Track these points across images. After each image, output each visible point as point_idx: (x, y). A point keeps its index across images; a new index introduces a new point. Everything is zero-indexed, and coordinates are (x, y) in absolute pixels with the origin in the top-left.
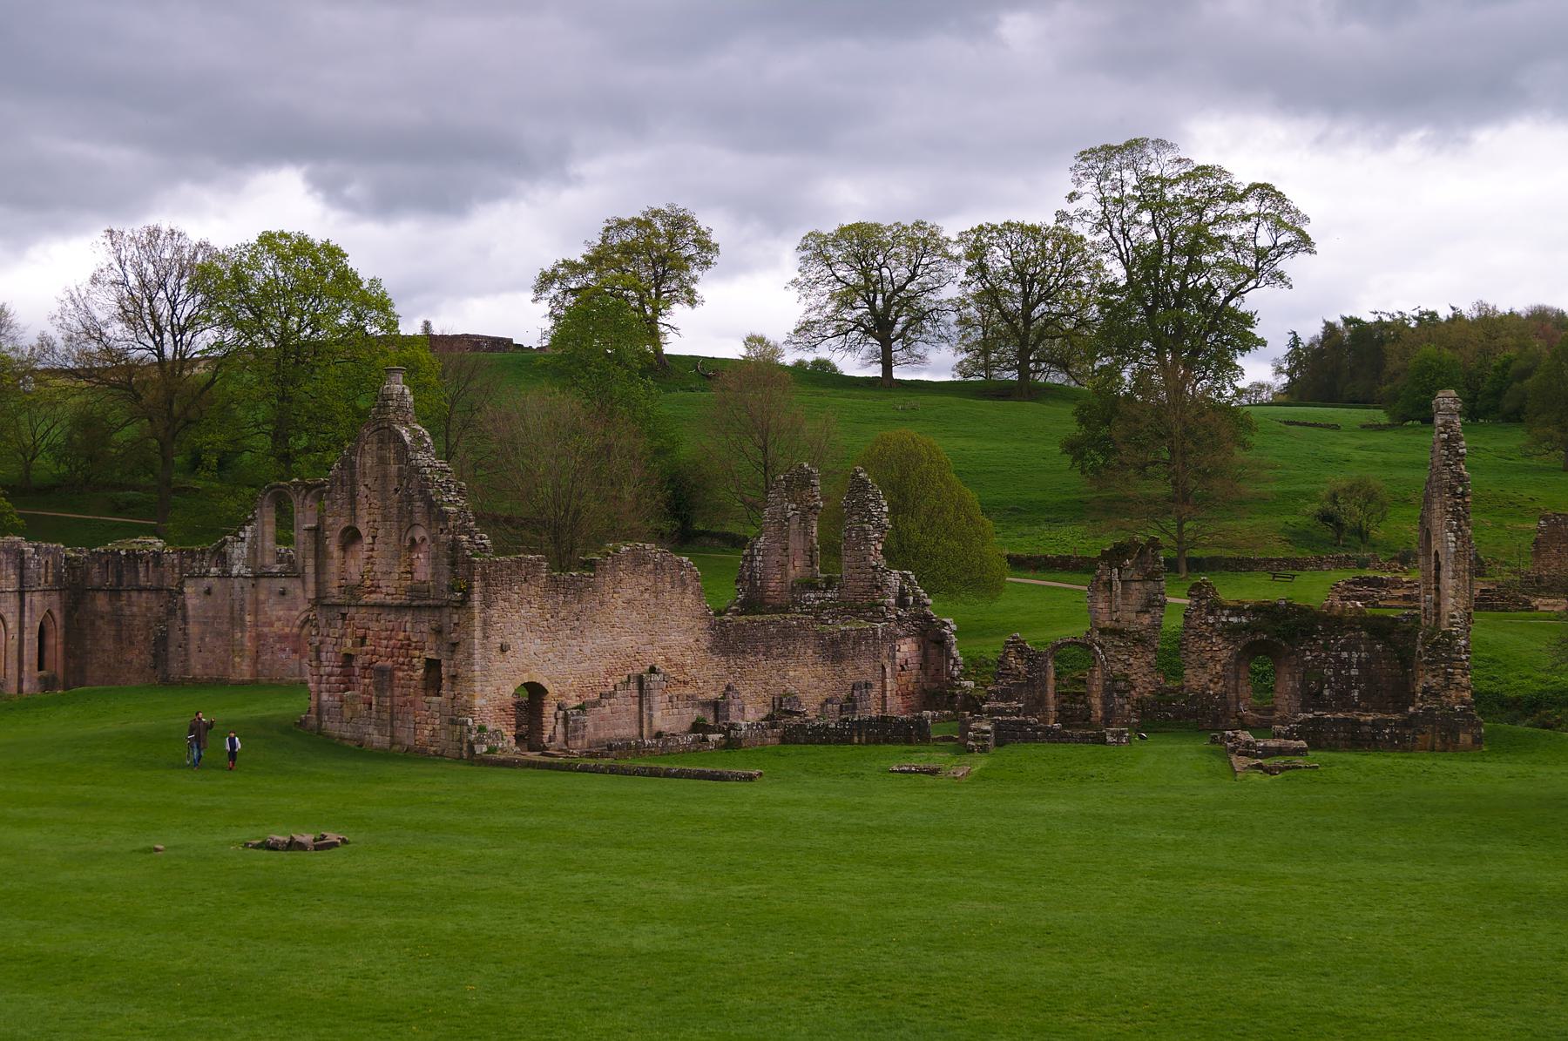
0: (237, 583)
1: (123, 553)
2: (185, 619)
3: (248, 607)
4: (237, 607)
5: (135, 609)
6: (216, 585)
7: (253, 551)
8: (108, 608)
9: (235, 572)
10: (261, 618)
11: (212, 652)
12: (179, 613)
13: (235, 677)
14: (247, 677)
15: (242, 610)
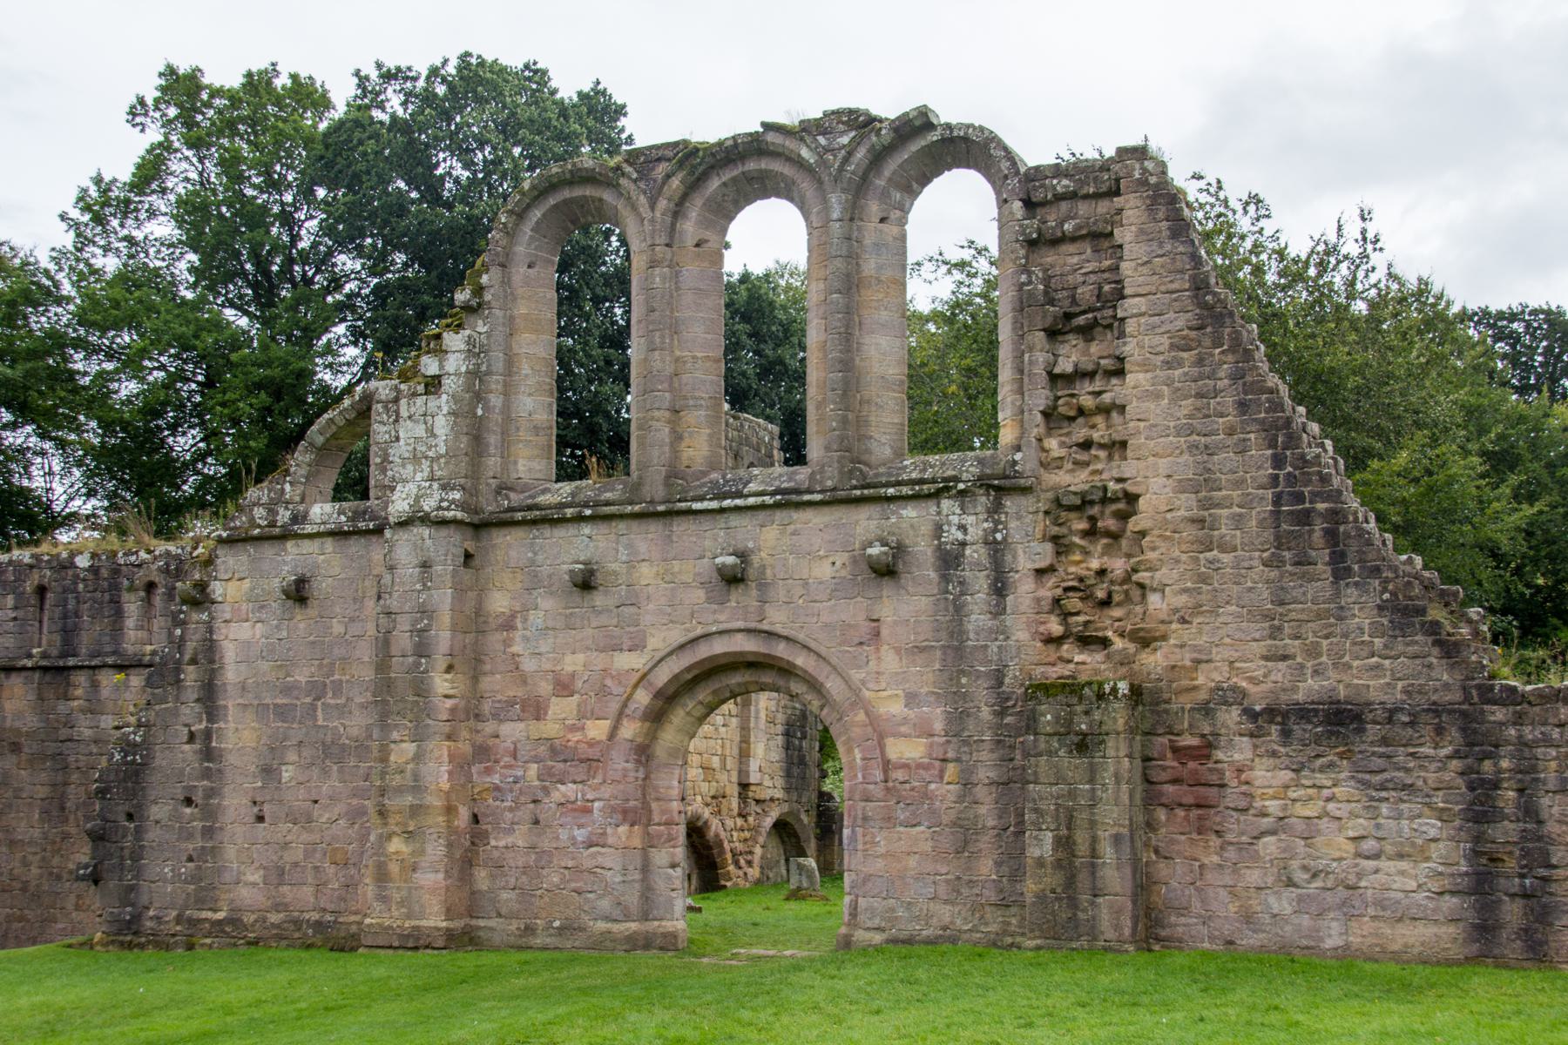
0: (406, 547)
1: (83, 562)
2: (209, 695)
3: (443, 638)
4: (403, 640)
5: (107, 722)
6: (326, 563)
7: (474, 433)
8: (31, 722)
9: (400, 505)
10: (496, 684)
11: (303, 819)
12: (190, 675)
14: (434, 920)
15: (422, 650)
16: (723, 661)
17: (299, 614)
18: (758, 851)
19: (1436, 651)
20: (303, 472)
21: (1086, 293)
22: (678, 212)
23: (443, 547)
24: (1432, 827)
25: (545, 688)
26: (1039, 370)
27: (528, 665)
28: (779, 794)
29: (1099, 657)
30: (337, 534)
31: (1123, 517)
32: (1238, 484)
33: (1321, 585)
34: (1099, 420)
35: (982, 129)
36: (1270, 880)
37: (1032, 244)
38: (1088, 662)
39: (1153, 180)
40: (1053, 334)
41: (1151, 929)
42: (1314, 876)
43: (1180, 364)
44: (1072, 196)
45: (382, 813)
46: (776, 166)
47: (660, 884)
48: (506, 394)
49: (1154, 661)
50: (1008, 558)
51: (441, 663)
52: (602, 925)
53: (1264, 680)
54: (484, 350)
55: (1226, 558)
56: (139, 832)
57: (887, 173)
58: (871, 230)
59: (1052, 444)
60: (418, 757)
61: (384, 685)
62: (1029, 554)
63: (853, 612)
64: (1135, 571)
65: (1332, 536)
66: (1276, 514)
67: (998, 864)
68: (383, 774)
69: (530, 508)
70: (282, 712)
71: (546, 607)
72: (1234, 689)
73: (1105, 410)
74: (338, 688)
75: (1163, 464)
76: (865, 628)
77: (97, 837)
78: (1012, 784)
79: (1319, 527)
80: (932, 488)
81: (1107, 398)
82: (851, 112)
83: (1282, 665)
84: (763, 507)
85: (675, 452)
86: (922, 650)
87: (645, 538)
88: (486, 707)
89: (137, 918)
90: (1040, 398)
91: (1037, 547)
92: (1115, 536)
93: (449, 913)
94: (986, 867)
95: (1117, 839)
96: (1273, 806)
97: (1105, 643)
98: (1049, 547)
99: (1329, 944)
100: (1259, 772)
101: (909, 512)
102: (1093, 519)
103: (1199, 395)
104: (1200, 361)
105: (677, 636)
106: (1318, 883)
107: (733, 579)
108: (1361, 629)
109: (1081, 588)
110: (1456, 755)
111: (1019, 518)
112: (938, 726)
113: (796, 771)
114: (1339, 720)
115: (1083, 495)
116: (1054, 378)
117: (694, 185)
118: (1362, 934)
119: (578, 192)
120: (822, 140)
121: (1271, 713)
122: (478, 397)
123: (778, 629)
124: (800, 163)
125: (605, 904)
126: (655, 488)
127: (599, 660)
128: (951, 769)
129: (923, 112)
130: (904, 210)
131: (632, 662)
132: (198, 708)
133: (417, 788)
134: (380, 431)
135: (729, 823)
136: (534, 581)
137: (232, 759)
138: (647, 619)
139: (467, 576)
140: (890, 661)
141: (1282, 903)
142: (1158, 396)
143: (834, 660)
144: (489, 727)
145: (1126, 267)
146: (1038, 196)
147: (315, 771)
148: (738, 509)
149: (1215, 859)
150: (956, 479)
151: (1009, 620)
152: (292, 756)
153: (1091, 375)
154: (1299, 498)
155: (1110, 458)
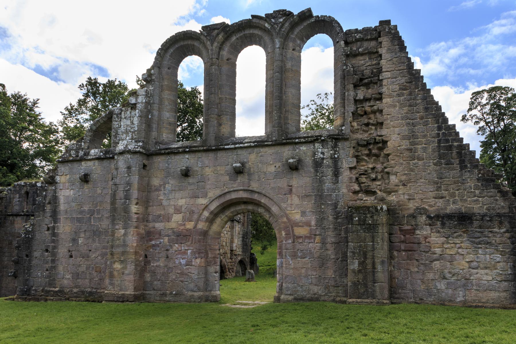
2: (55, 215)
3: (135, 194)
4: (121, 194)
9: (120, 147)
11: (86, 257)
12: (48, 208)
13: (110, 290)
14: (130, 292)
15: (127, 197)
16: (235, 201)
17: (86, 186)
18: (235, 268)
19: (499, 195)
20: (88, 138)
21: (367, 72)
22: (221, 48)
23: (136, 161)
24: (498, 257)
25: (171, 210)
26: (351, 98)
27: (165, 203)
28: (240, 253)
29: (373, 198)
30: (99, 159)
31: (381, 149)
32: (425, 136)
33: (456, 172)
34: (372, 116)
35: (330, 17)
36: (437, 277)
37: (347, 56)
38: (369, 200)
39: (393, 32)
40: (356, 86)
41: (394, 295)
42: (453, 275)
43: (403, 95)
44: (361, 40)
45: (112, 254)
46: (256, 32)
47: (211, 279)
48: (160, 110)
49: (392, 198)
50: (340, 163)
51: (134, 202)
52: (190, 293)
53: (435, 205)
54: (152, 96)
55: (420, 163)
56: (30, 261)
57: (295, 33)
58: (290, 53)
59: (355, 124)
60: (125, 235)
61: (114, 210)
62: (347, 162)
63: (283, 183)
64: (385, 168)
65: (459, 154)
66: (439, 146)
67: (335, 272)
68: (113, 240)
69: (167, 149)
70: (79, 220)
71: (172, 183)
72: (424, 209)
73: (374, 112)
74: (99, 212)
75: (397, 130)
76: (287, 188)
77: (17, 263)
78: (342, 243)
79: (455, 151)
80: (312, 139)
81: (375, 108)
82: (283, 10)
83: (441, 200)
84: (250, 147)
85: (219, 131)
86: (307, 196)
87: (207, 159)
88: (150, 218)
89: (29, 290)
90: (351, 108)
91: (350, 159)
92: (377, 156)
93: (135, 289)
94: (330, 273)
95: (383, 262)
96: (438, 251)
97: (374, 193)
98: (355, 159)
99: (459, 299)
100: (434, 239)
101: (303, 148)
102: (370, 150)
103: (410, 106)
104: (410, 94)
105: (218, 192)
106: (455, 278)
107: (239, 172)
108: (471, 187)
109: (365, 173)
110: (507, 232)
111: (344, 149)
112: (313, 223)
113: (245, 247)
114: (463, 220)
115: (367, 141)
116: (356, 101)
117: (227, 38)
118: (472, 296)
119: (186, 43)
120: (273, 20)
121: (438, 217)
122: (149, 112)
123: (255, 189)
124: (265, 30)
125: (192, 286)
126: (212, 142)
127: (192, 201)
128: (318, 238)
129: (309, 10)
130: (301, 48)
131: (203, 201)
132: (51, 219)
133: (125, 245)
134: (115, 124)
135: (228, 261)
136: (168, 174)
137: (62, 236)
138: (208, 187)
139: (144, 172)
140: (296, 200)
141: (442, 285)
142: (395, 106)
143: (275, 200)
144: (151, 225)
145: (383, 62)
146: (350, 39)
147: (91, 240)
148: (241, 148)
149: (416, 269)
150: (321, 136)
151: (339, 185)
152: (82, 235)
153: (369, 100)
154: (447, 141)
155: (376, 129)
